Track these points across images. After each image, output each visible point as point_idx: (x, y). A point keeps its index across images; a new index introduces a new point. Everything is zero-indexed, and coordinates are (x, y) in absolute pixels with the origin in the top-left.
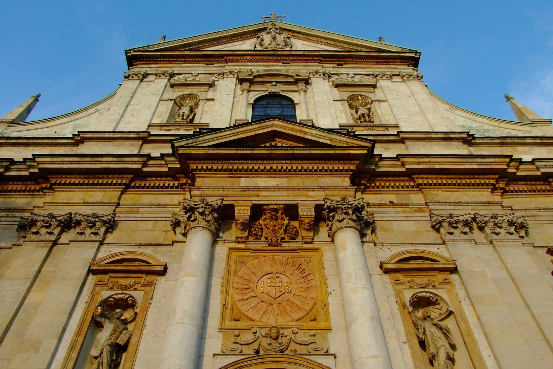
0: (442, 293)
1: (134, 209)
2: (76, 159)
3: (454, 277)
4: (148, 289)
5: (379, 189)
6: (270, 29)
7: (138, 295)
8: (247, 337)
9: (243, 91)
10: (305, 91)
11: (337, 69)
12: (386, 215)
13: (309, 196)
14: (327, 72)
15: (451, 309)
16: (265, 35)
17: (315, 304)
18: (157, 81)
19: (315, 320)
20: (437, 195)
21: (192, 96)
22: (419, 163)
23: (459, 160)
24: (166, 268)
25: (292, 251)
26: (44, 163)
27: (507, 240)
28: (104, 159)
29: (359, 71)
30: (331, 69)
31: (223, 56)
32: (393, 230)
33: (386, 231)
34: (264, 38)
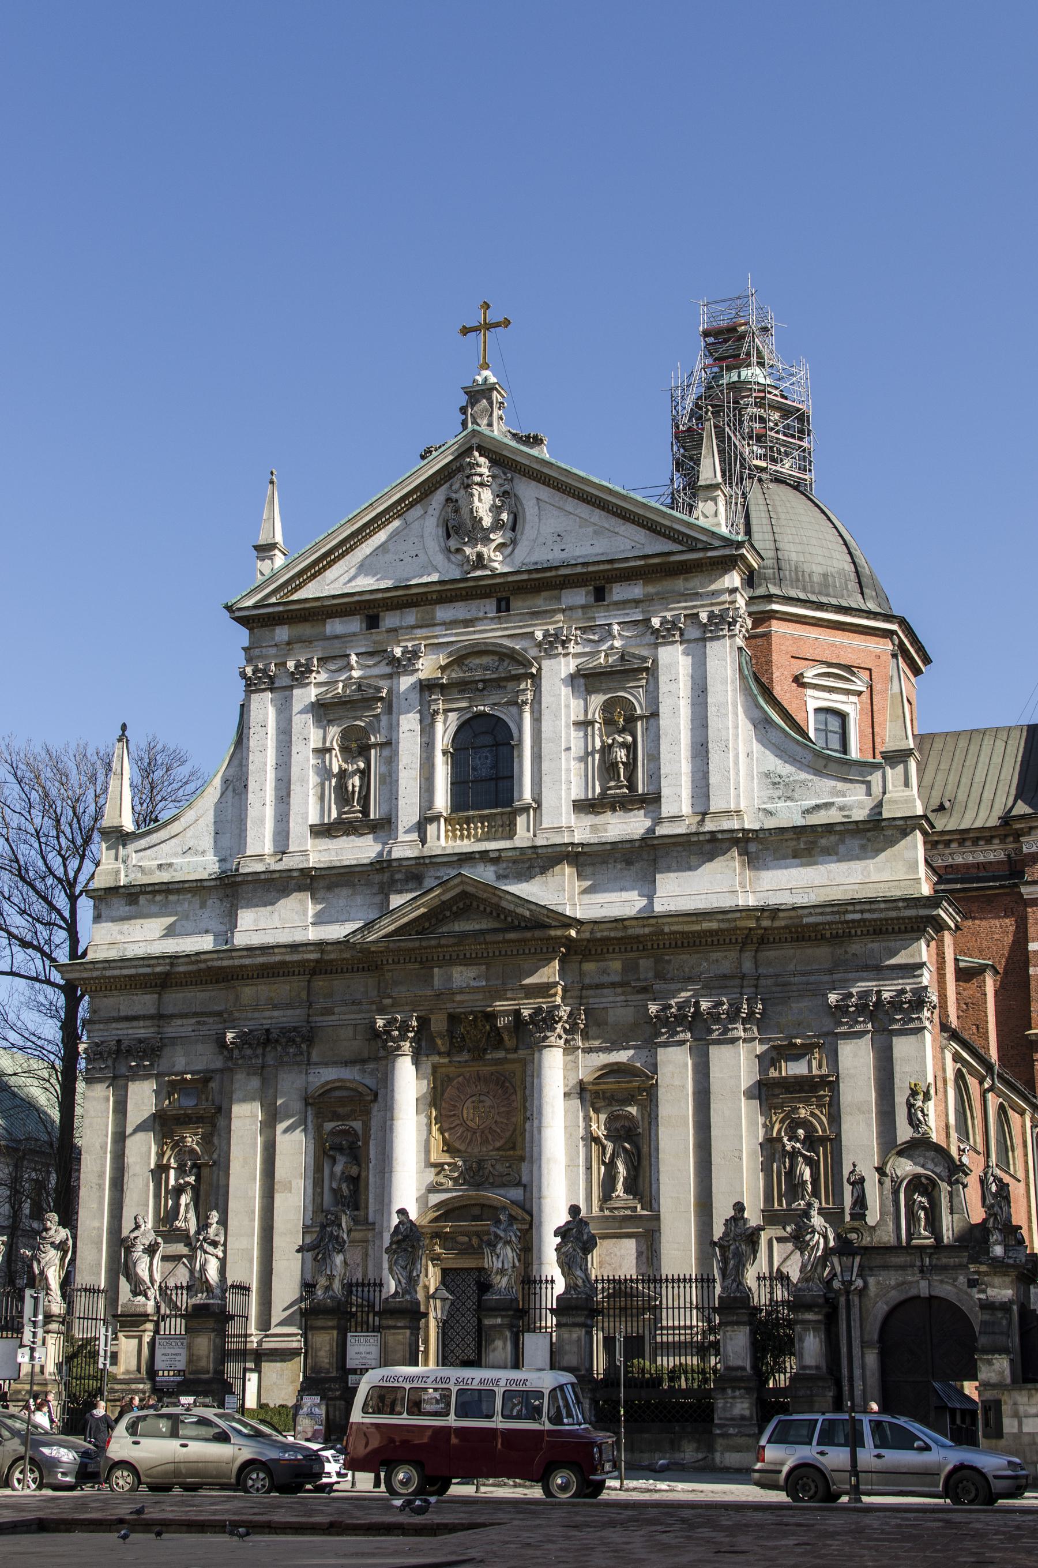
1: (328, 1011)
2: (245, 953)
4: (365, 1118)
6: (468, 477)
7: (357, 1125)
12: (604, 1000)
15: (640, 1130)
16: (463, 492)
17: (515, 1130)
19: (513, 1148)
20: (669, 962)
22: (644, 926)
23: (694, 918)
24: (376, 1095)
26: (212, 960)
28: (276, 950)
29: (628, 614)
32: (606, 1024)
33: (599, 1025)
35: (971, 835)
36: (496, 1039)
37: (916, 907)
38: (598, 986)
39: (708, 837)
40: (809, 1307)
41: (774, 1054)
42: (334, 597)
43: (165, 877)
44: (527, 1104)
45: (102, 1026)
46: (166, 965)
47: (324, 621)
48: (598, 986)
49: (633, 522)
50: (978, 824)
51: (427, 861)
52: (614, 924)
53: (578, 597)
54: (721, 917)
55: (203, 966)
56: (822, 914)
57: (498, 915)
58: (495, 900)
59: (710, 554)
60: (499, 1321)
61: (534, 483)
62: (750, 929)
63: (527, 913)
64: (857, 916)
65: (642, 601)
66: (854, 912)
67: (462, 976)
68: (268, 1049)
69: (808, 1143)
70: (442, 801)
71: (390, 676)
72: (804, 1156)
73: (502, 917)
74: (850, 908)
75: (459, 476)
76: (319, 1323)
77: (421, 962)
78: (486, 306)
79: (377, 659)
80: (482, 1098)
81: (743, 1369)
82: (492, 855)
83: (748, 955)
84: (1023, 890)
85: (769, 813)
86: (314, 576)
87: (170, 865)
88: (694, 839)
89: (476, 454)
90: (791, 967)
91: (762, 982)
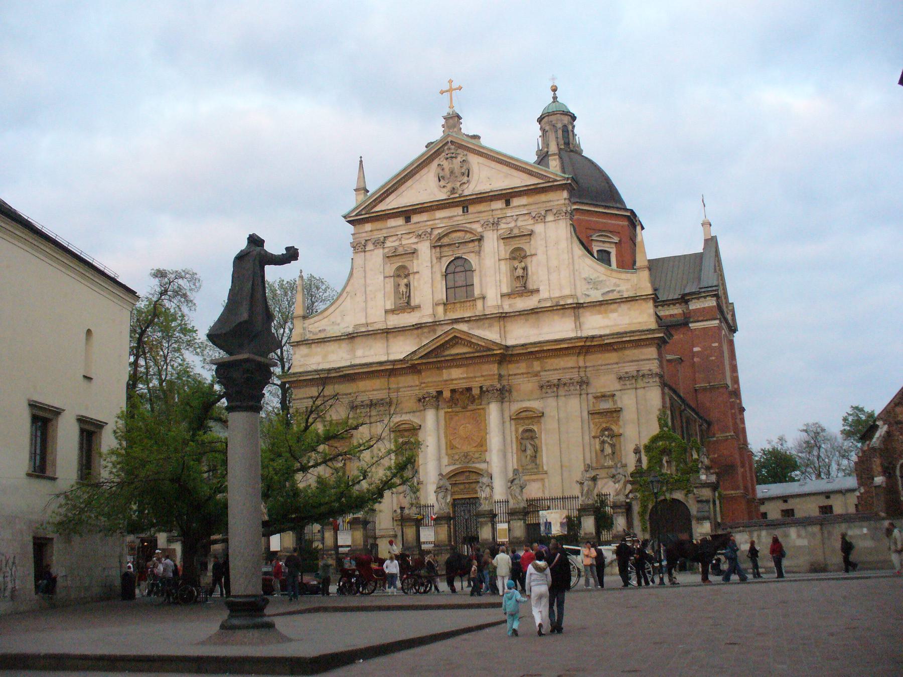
0: (535, 428)
3: (543, 419)
5: (517, 362)
8: (457, 457)
9: (437, 259)
10: (479, 252)
11: (504, 211)
13: (476, 382)
14: (496, 220)
16: (445, 161)
18: (375, 251)
21: (403, 267)
24: (420, 426)
25: (472, 410)
27: (572, 395)
30: (499, 212)
31: (416, 209)
34: (444, 166)
35: (668, 303)
36: (473, 400)
37: (653, 334)
38: (515, 375)
39: (561, 307)
40: (619, 507)
41: (594, 400)
42: (391, 209)
43: (322, 335)
44: (487, 427)
45: (299, 401)
46: (325, 374)
47: (386, 220)
48: (515, 375)
49: (521, 171)
50: (670, 298)
51: (438, 323)
52: (523, 347)
53: (499, 204)
54: (568, 341)
55: (341, 374)
56: (613, 338)
57: (471, 346)
58: (469, 339)
59: (556, 183)
60: (485, 519)
61: (476, 156)
62: (582, 346)
63: (483, 344)
64: (628, 339)
65: (526, 205)
66: (626, 337)
67: (456, 373)
68: (372, 408)
69: (610, 437)
70: (441, 295)
71: (417, 243)
72: (609, 443)
73: (472, 346)
74: (625, 335)
75: (443, 154)
76: (407, 524)
77: (437, 368)
78: (451, 81)
79: (411, 235)
80: (468, 425)
81: (592, 534)
82: (466, 319)
83: (581, 358)
84: (690, 325)
85: (588, 296)
86: (381, 201)
87: (325, 330)
88: (555, 308)
89: (450, 144)
90: (600, 362)
91: (588, 369)
